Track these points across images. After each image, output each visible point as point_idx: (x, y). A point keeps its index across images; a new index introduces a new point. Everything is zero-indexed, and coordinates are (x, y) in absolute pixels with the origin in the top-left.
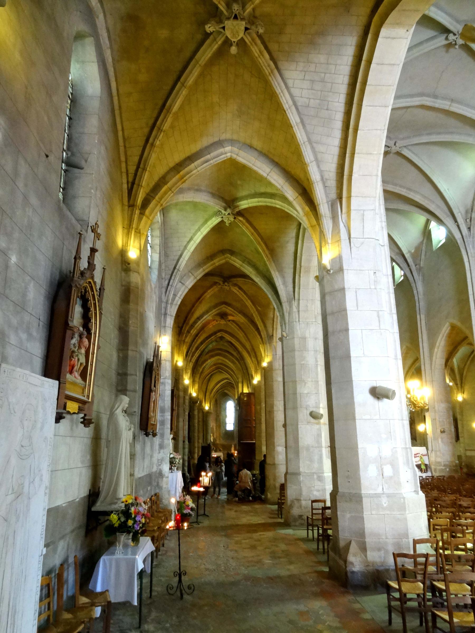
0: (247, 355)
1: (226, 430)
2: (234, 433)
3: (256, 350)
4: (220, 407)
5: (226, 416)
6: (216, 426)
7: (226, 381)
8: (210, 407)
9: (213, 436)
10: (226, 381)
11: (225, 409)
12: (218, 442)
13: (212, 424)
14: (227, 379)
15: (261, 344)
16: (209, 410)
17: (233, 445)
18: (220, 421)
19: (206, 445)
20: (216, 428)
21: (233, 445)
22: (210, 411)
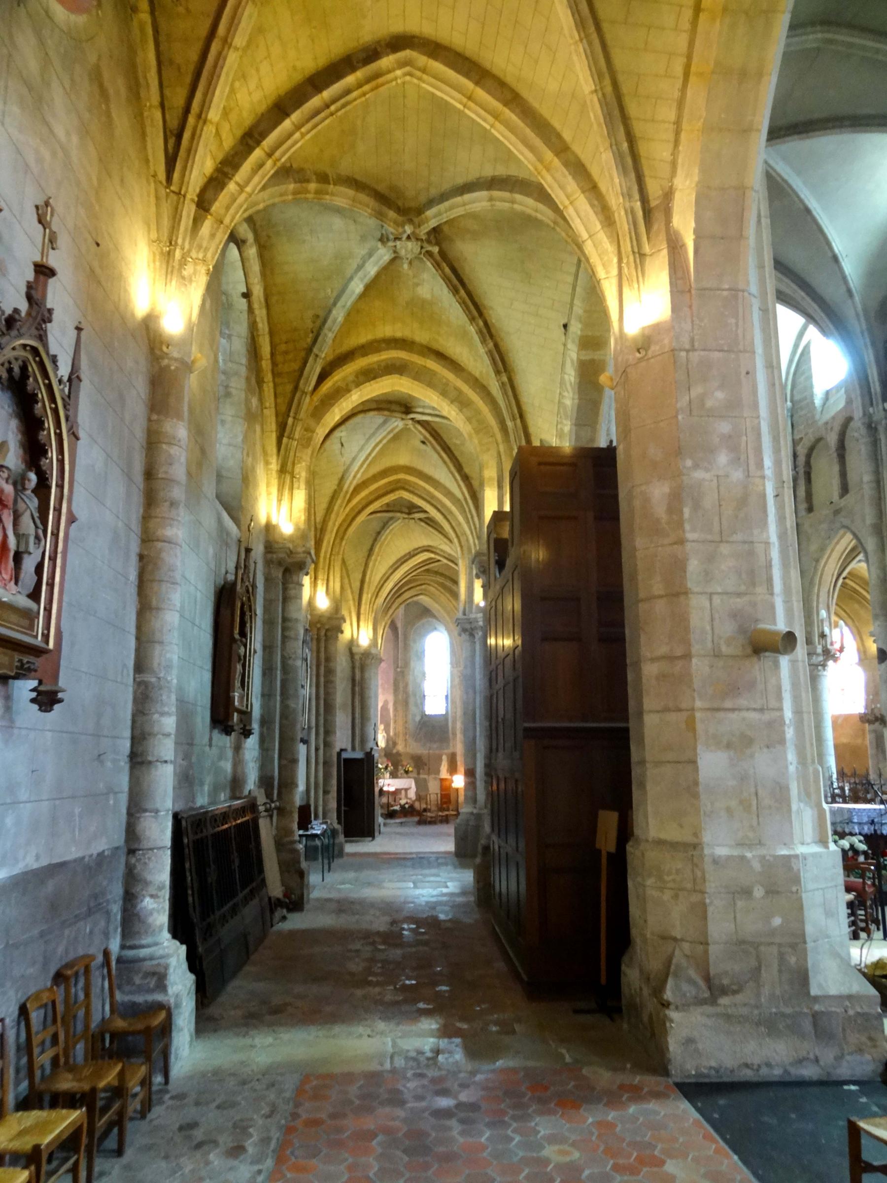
0: (572, 185)
1: (423, 715)
2: (447, 720)
3: (638, 128)
4: (406, 647)
5: (424, 674)
6: (395, 704)
7: (426, 556)
9: (387, 730)
10: (426, 556)
11: (420, 656)
12: (400, 748)
13: (382, 697)
14: (427, 549)
16: (370, 646)
17: (444, 758)
18: (406, 686)
19: (359, 755)
20: (395, 710)
22: (373, 651)
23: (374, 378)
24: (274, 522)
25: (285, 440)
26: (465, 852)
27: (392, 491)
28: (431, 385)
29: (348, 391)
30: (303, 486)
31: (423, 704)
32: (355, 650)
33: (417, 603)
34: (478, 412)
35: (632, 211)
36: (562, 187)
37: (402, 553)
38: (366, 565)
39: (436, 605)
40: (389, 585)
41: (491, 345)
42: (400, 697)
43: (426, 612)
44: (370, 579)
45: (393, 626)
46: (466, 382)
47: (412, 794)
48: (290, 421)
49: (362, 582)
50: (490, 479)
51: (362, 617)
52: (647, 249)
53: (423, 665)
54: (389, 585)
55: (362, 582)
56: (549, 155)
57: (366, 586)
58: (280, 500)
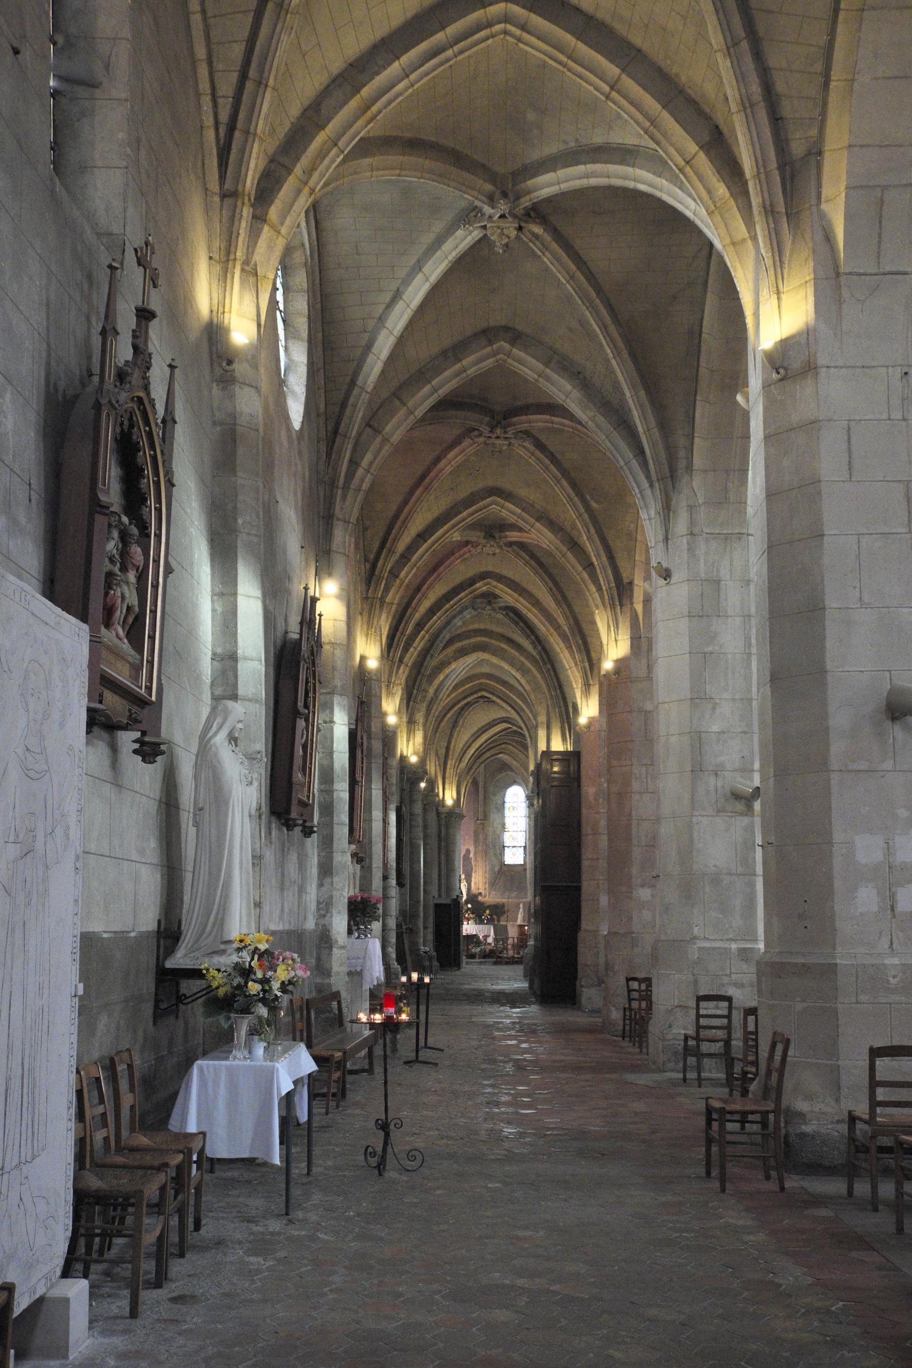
3: (587, 632)
5: (503, 825)
8: (457, 801)
10: (505, 725)
11: (501, 808)
15: (598, 608)
17: (521, 906)
19: (448, 901)
21: (521, 906)
23: (466, 654)
24: (405, 754)
25: (411, 703)
26: (530, 975)
27: (476, 692)
28: (503, 659)
29: (450, 663)
30: (421, 728)
31: (502, 854)
32: (441, 809)
33: (499, 759)
34: (535, 677)
35: (585, 667)
36: (558, 644)
37: (483, 724)
38: (451, 735)
39: (515, 763)
40: (471, 751)
41: (540, 648)
42: (480, 848)
43: (505, 767)
44: (455, 746)
45: (475, 783)
46: (527, 658)
47: (490, 940)
48: (415, 691)
49: (448, 748)
50: (542, 723)
51: (447, 781)
52: (591, 682)
53: (503, 817)
54: (471, 751)
55: (448, 748)
56: (552, 630)
57: (451, 752)
58: (408, 741)
